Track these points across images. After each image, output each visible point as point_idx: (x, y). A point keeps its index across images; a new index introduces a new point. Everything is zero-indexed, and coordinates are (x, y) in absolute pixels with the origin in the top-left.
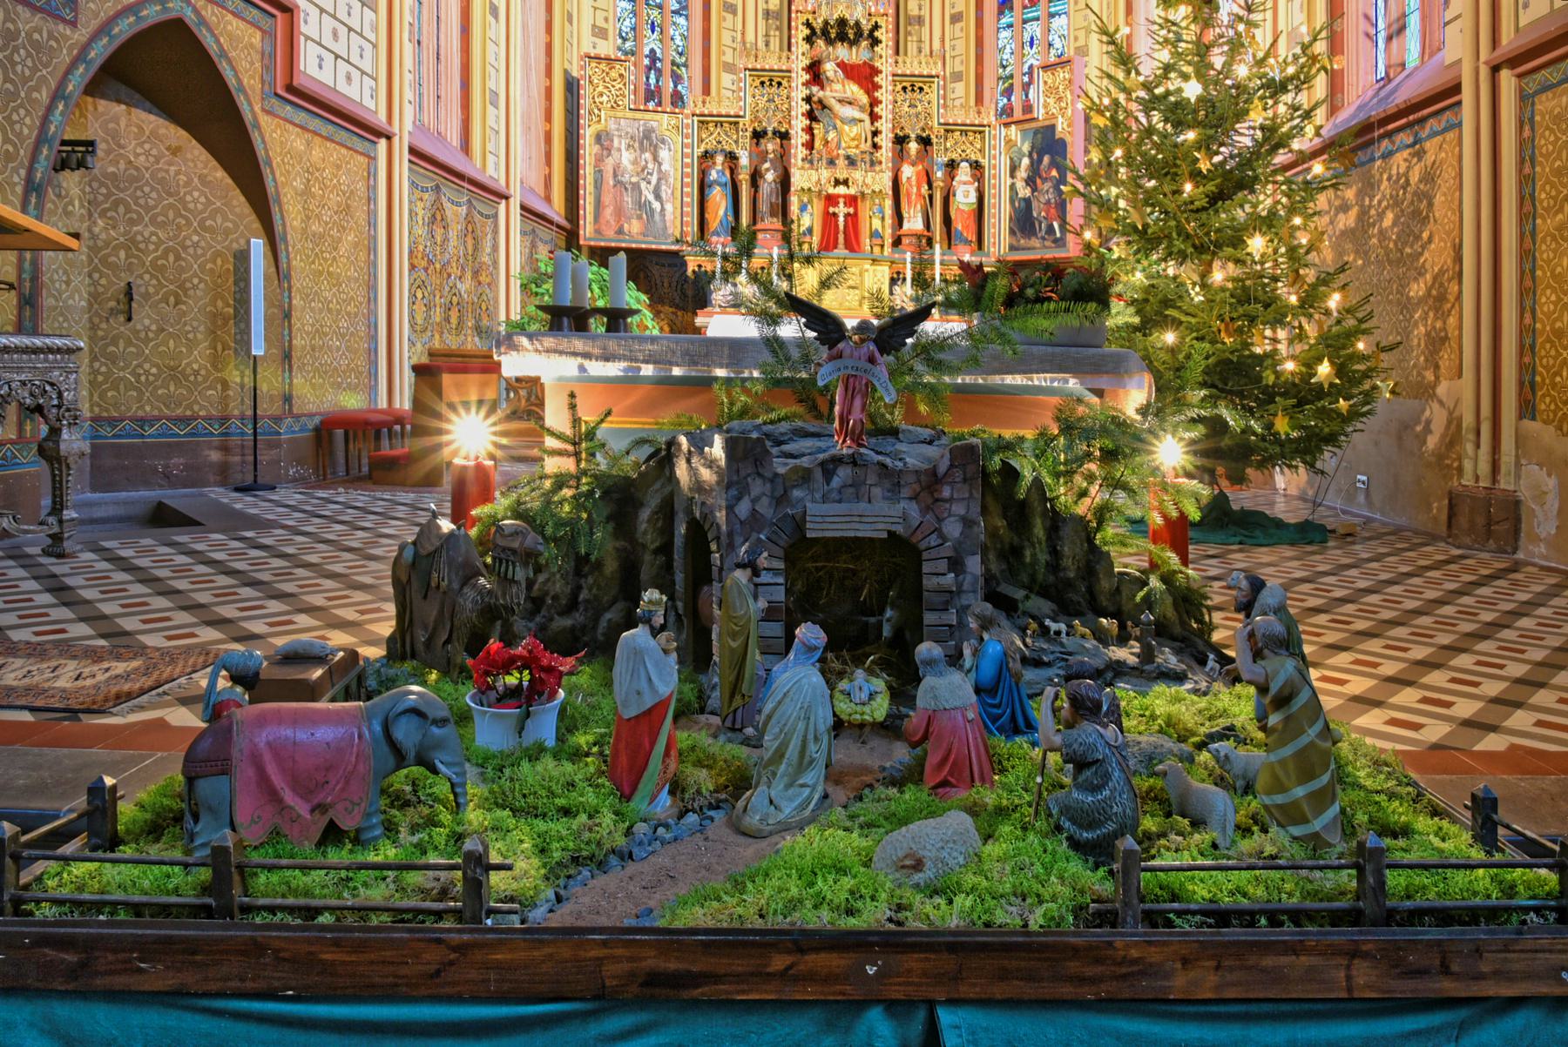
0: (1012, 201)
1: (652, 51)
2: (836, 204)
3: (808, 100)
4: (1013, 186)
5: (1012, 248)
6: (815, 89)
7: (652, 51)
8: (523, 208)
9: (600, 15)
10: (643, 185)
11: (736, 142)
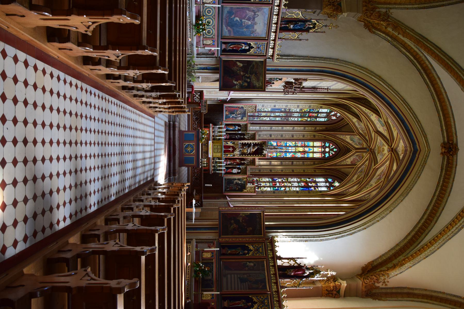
0: (233, 179)
1: (262, 114)
2: (232, 148)
3: (250, 143)
4: (236, 179)
5: (225, 179)
6: (252, 144)
7: (262, 114)
8: (227, 98)
9: (266, 106)
10: (235, 115)
11: (243, 131)
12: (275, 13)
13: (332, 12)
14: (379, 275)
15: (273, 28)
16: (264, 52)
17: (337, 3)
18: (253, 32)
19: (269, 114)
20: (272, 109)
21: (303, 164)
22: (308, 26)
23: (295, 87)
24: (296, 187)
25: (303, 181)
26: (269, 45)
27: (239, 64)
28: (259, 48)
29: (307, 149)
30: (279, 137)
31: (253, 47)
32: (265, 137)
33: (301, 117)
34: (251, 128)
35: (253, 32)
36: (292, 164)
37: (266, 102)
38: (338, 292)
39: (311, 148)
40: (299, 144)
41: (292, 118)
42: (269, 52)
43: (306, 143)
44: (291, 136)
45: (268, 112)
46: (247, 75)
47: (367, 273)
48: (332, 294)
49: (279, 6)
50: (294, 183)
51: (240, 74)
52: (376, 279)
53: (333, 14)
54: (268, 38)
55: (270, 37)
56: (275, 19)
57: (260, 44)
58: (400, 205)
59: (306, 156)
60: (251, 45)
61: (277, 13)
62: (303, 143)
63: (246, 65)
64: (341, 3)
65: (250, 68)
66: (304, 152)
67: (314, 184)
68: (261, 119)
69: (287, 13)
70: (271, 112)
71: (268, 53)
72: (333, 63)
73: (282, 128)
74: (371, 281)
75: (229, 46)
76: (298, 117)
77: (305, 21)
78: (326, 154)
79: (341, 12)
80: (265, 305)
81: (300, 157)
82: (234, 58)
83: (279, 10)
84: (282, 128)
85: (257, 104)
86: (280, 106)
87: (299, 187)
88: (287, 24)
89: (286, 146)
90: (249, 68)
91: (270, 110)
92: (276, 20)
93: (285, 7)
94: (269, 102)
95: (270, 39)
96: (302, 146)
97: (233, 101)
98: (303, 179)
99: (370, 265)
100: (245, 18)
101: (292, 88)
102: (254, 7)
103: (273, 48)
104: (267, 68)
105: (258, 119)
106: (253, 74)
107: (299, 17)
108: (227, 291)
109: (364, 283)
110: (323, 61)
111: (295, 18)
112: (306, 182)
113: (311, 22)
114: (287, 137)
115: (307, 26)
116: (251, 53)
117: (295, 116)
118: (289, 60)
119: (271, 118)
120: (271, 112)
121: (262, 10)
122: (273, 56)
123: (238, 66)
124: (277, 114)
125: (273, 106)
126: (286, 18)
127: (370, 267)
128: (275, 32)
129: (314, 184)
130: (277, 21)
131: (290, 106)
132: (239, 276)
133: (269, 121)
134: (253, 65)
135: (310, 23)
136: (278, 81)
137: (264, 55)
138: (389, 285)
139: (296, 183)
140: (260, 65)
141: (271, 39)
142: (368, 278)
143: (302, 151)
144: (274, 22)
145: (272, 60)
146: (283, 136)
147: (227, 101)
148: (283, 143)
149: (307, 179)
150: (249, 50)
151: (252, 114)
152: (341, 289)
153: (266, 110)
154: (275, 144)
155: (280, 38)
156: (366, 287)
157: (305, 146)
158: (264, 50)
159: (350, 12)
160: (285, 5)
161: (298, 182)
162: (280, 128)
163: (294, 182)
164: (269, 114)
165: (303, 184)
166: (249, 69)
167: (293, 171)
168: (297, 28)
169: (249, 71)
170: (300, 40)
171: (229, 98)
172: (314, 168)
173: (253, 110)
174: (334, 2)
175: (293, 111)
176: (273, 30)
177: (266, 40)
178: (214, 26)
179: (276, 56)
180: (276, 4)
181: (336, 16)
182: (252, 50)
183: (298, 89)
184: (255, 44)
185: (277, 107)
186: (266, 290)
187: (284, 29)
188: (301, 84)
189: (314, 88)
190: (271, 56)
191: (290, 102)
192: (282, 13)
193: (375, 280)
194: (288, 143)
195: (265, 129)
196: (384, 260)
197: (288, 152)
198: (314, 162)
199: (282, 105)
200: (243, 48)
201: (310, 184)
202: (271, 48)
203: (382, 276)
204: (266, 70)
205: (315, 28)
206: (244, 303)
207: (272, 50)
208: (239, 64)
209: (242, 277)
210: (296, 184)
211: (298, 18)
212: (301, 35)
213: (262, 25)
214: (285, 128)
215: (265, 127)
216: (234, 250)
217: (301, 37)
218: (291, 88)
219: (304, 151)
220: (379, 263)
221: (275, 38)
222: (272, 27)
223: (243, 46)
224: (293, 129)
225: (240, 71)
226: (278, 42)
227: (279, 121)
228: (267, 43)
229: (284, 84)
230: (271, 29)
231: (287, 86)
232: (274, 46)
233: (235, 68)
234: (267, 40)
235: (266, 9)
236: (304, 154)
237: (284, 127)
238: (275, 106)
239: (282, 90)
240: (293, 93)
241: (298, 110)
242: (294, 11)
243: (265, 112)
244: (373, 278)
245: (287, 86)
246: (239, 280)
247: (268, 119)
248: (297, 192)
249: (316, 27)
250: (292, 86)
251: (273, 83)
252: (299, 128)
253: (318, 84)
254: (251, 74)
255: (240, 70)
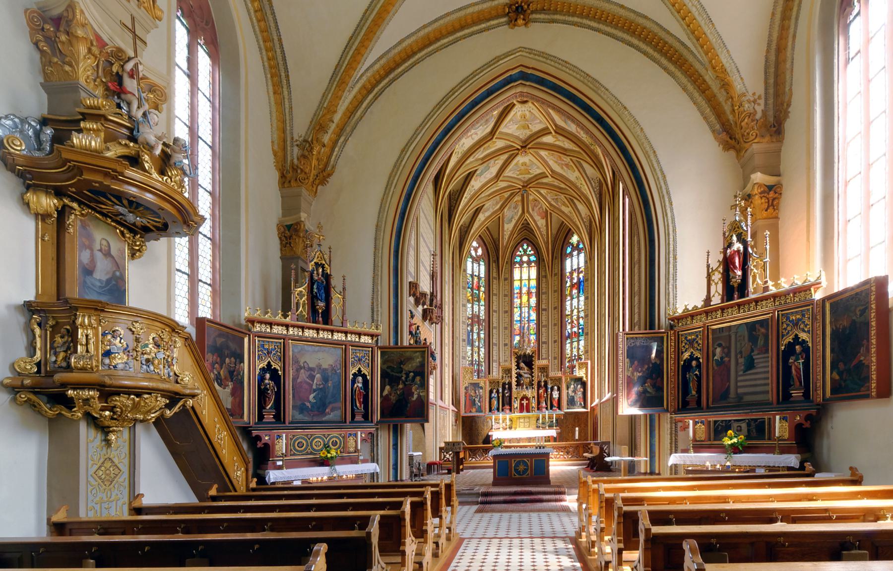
12: (300, 334)
13: (301, 240)
14: (740, 113)
15: (322, 335)
16: (366, 351)
17: (287, 232)
18: (333, 369)
19: (476, 349)
20: (468, 344)
21: (545, 293)
22: (320, 276)
23: (431, 305)
24: (579, 301)
25: (570, 291)
26: (355, 342)
27: (386, 393)
28: (360, 360)
29: (524, 290)
30: (508, 332)
31: (360, 369)
32: (508, 353)
33: (479, 301)
34: (496, 374)
35: (333, 369)
36: (545, 310)
37: (457, 353)
38: (770, 188)
39: (523, 283)
40: (517, 301)
41: (481, 315)
42: (366, 342)
43: (516, 291)
44: (506, 314)
45: (472, 350)
46: (403, 378)
47: (734, 141)
48: (774, 199)
49: (287, 326)
50: (574, 305)
51: (402, 389)
52: (747, 117)
53: (304, 237)
54: (342, 345)
55: (341, 341)
56: (310, 333)
57: (354, 358)
58: (614, 92)
59: (534, 290)
60: (355, 373)
61: (300, 330)
62: (516, 295)
63: (387, 380)
64: (286, 226)
65: (391, 373)
66: (529, 293)
67: (575, 275)
68: (482, 360)
69: (298, 312)
70: (472, 346)
71: (368, 343)
72: (382, 234)
73: (495, 328)
74: (752, 127)
75: (358, 409)
76: (479, 305)
77: (312, 282)
78: (532, 260)
79: (299, 223)
80: (802, 319)
81: (535, 299)
82: (377, 400)
83: (294, 326)
84: (495, 328)
85: (461, 366)
86: (464, 333)
87: (578, 297)
88: (318, 312)
89: (520, 321)
90: (392, 375)
91: (469, 348)
92: (311, 331)
93: (288, 316)
94: (457, 348)
95: (343, 341)
96: (521, 297)
97: (456, 402)
98: (568, 292)
99: (720, 136)
100: (310, 383)
101: (432, 309)
102: (291, 369)
103: (359, 334)
104: (392, 344)
105: (482, 366)
106: (401, 368)
107: (305, 292)
108: (770, 392)
109: (756, 141)
110: (380, 252)
111: (307, 299)
112: (572, 286)
113: (313, 270)
114: (507, 320)
115: (319, 279)
116: (369, 373)
117: (477, 310)
118: (379, 309)
119: (481, 346)
120: (472, 346)
121: (296, 357)
122: (372, 336)
123: (390, 394)
124: (475, 336)
125: (464, 343)
126: (308, 314)
127: (724, 136)
128: (332, 331)
129: (575, 275)
130: (313, 329)
131: (464, 318)
132: (741, 373)
133: (485, 348)
134: (388, 367)
135: (315, 272)
136: (420, 333)
137: (372, 351)
138: (760, 90)
139: (573, 302)
140: (387, 357)
141: (344, 338)
142: (745, 134)
143: (527, 297)
144: (315, 335)
145: (379, 337)
146: (506, 326)
147: (456, 410)
148: (517, 326)
149: (568, 284)
150: (364, 376)
151: (475, 374)
152: (766, 184)
153: (469, 353)
154: (517, 338)
155: (342, 323)
156: (763, 136)
157: (521, 293)
158: (362, 350)
159: (300, 209)
160: (285, 316)
161: (572, 299)
162: (494, 331)
163: (571, 304)
164: (476, 349)
165: (575, 291)
166: (394, 374)
167: (555, 308)
168: (324, 295)
169: (397, 375)
170: (344, 289)
171: (452, 408)
172: (552, 276)
173: (469, 372)
174: (285, 236)
175: (471, 313)
176: (330, 337)
177: (345, 348)
178: (324, 435)
179: (373, 330)
180: (285, 332)
181: (310, 233)
182: (365, 371)
183: (435, 301)
184: (353, 364)
185: (465, 337)
186: (770, 321)
187: (327, 317)
188: (424, 295)
189: (433, 277)
190: (372, 339)
191: (458, 317)
192: (298, 320)
193: (750, 120)
194: (515, 319)
195: (496, 353)
196: (711, 110)
197: (529, 317)
198: (542, 277)
199: (462, 330)
200: (360, 385)
201: (575, 281)
202: (359, 339)
203: (743, 107)
204: (397, 346)
205: (324, 265)
206: (797, 359)
207: (362, 337)
208: (386, 393)
209: (743, 367)
210: (575, 301)
211: (308, 293)
212: (336, 289)
213: (320, 355)
214: (495, 325)
215: (494, 353)
216: (691, 385)
217: (339, 288)
218: (432, 312)
219: (528, 293)
220: (716, 119)
221: (341, 332)
222: (323, 338)
223: (357, 386)
224: (495, 311)
225: (397, 389)
226: (349, 327)
227: (485, 334)
228: (352, 346)
229: (427, 323)
230: (327, 339)
231: (429, 318)
232: (355, 333)
233: (393, 398)
234: (345, 345)
235: (292, 349)
236: (531, 293)
237: (494, 325)
238: (464, 340)
239: (438, 326)
240: (441, 307)
241: (469, 305)
242: (296, 301)
243: (472, 354)
244: (747, 124)
245: (429, 318)
246: (746, 373)
247: (482, 350)
248: (586, 298)
249: (321, 264)
250: (429, 309)
251: (425, 340)
252: (495, 304)
253: (426, 269)
254: (402, 372)
255: (395, 390)
